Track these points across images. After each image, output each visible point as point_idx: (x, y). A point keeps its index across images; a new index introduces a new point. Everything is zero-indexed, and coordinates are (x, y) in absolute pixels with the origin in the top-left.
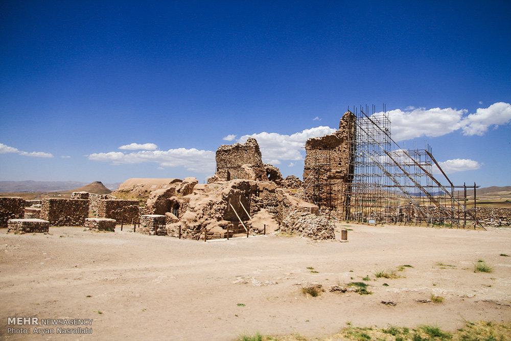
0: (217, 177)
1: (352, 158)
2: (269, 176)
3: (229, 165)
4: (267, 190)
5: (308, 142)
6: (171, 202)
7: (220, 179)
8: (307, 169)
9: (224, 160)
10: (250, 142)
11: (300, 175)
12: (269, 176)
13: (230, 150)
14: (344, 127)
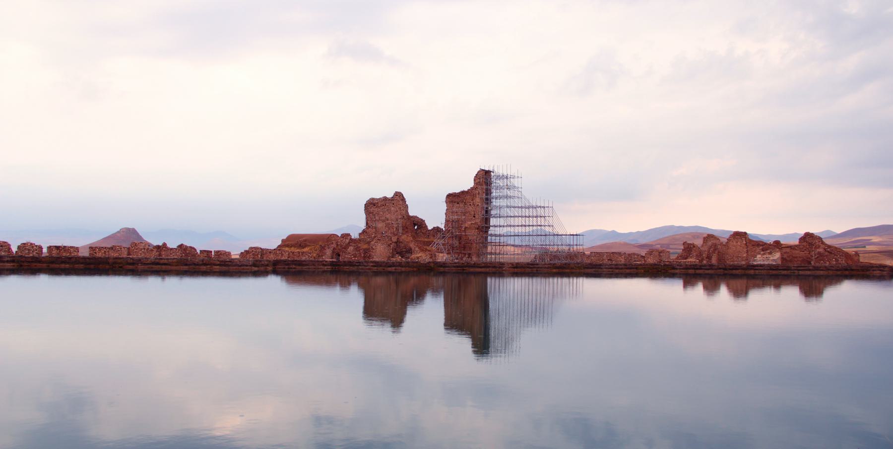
1: (487, 212)
2: (416, 227)
8: (447, 221)
13: (378, 203)
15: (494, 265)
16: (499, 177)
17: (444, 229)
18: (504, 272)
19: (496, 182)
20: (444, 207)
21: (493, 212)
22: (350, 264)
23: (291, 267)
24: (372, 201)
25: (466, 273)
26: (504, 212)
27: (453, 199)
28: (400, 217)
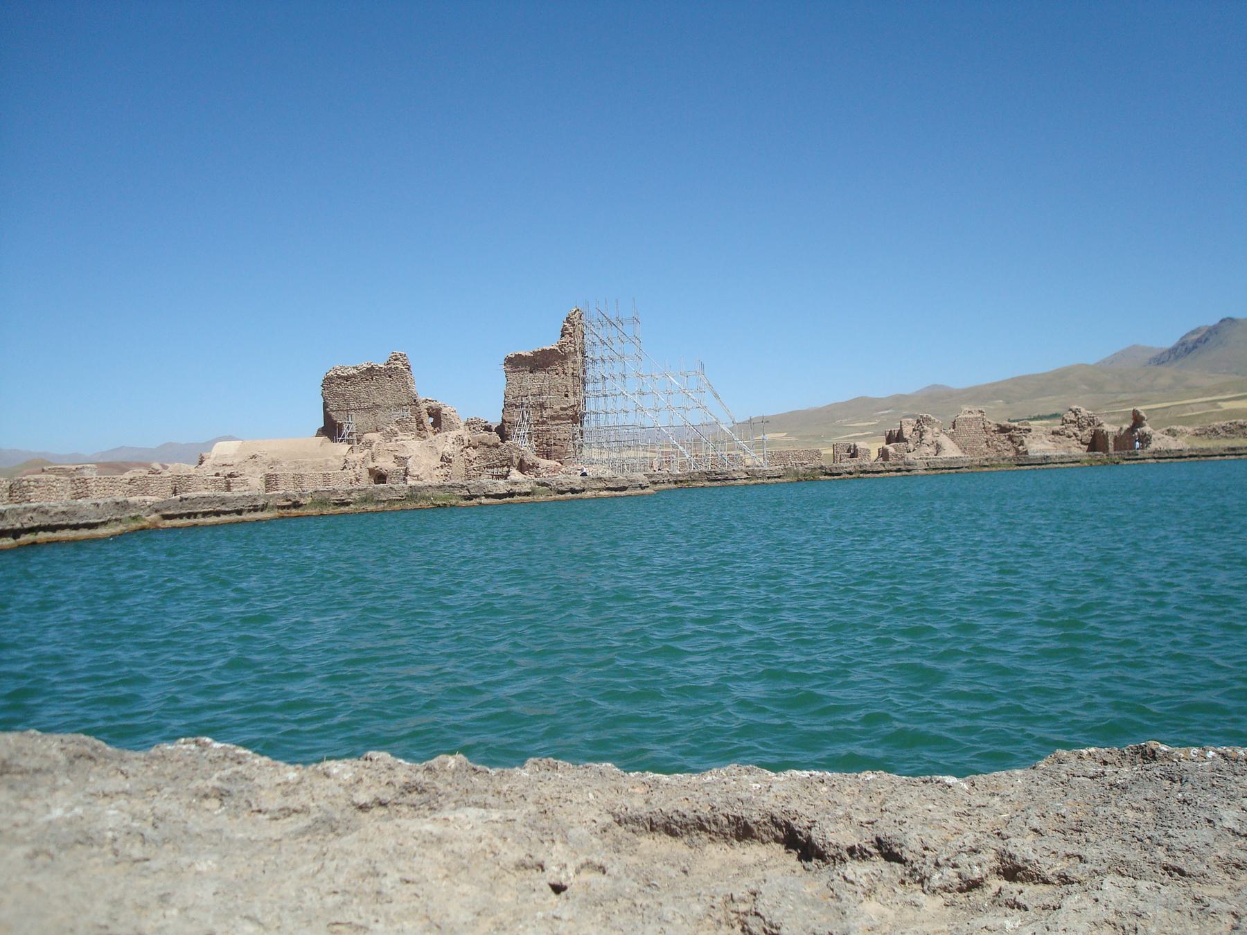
0: (396, 429)
4: (485, 444)
5: (509, 361)
6: (371, 471)
7: (400, 433)
10: (395, 360)
13: (354, 376)
14: (570, 334)
15: (898, 467)
27: (515, 363)
28: (406, 401)
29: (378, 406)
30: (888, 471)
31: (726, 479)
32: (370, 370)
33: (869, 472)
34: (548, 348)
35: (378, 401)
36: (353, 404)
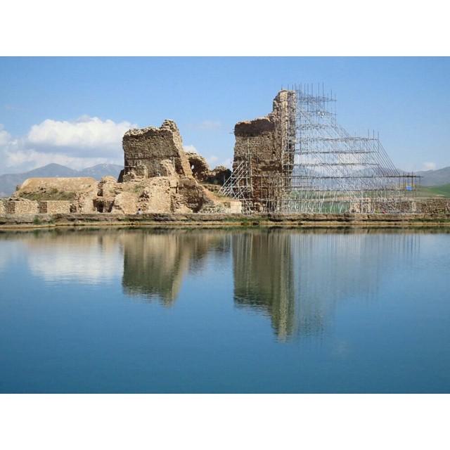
3: (140, 155)
9: (135, 148)
11: (228, 164)
12: (193, 167)
14: (277, 109)
16: (309, 100)
17: (232, 170)
18: (353, 226)
19: (301, 108)
20: (232, 140)
21: (297, 147)
22: (156, 217)
23: (77, 223)
24: (133, 133)
25: (304, 228)
26: (313, 146)
27: (243, 131)
28: (172, 154)
29: (155, 157)
30: (331, 220)
31: (167, 220)
32: (151, 131)
33: (311, 220)
34: (261, 118)
35: (155, 153)
36: (140, 155)
